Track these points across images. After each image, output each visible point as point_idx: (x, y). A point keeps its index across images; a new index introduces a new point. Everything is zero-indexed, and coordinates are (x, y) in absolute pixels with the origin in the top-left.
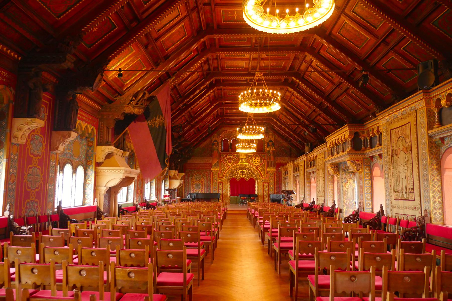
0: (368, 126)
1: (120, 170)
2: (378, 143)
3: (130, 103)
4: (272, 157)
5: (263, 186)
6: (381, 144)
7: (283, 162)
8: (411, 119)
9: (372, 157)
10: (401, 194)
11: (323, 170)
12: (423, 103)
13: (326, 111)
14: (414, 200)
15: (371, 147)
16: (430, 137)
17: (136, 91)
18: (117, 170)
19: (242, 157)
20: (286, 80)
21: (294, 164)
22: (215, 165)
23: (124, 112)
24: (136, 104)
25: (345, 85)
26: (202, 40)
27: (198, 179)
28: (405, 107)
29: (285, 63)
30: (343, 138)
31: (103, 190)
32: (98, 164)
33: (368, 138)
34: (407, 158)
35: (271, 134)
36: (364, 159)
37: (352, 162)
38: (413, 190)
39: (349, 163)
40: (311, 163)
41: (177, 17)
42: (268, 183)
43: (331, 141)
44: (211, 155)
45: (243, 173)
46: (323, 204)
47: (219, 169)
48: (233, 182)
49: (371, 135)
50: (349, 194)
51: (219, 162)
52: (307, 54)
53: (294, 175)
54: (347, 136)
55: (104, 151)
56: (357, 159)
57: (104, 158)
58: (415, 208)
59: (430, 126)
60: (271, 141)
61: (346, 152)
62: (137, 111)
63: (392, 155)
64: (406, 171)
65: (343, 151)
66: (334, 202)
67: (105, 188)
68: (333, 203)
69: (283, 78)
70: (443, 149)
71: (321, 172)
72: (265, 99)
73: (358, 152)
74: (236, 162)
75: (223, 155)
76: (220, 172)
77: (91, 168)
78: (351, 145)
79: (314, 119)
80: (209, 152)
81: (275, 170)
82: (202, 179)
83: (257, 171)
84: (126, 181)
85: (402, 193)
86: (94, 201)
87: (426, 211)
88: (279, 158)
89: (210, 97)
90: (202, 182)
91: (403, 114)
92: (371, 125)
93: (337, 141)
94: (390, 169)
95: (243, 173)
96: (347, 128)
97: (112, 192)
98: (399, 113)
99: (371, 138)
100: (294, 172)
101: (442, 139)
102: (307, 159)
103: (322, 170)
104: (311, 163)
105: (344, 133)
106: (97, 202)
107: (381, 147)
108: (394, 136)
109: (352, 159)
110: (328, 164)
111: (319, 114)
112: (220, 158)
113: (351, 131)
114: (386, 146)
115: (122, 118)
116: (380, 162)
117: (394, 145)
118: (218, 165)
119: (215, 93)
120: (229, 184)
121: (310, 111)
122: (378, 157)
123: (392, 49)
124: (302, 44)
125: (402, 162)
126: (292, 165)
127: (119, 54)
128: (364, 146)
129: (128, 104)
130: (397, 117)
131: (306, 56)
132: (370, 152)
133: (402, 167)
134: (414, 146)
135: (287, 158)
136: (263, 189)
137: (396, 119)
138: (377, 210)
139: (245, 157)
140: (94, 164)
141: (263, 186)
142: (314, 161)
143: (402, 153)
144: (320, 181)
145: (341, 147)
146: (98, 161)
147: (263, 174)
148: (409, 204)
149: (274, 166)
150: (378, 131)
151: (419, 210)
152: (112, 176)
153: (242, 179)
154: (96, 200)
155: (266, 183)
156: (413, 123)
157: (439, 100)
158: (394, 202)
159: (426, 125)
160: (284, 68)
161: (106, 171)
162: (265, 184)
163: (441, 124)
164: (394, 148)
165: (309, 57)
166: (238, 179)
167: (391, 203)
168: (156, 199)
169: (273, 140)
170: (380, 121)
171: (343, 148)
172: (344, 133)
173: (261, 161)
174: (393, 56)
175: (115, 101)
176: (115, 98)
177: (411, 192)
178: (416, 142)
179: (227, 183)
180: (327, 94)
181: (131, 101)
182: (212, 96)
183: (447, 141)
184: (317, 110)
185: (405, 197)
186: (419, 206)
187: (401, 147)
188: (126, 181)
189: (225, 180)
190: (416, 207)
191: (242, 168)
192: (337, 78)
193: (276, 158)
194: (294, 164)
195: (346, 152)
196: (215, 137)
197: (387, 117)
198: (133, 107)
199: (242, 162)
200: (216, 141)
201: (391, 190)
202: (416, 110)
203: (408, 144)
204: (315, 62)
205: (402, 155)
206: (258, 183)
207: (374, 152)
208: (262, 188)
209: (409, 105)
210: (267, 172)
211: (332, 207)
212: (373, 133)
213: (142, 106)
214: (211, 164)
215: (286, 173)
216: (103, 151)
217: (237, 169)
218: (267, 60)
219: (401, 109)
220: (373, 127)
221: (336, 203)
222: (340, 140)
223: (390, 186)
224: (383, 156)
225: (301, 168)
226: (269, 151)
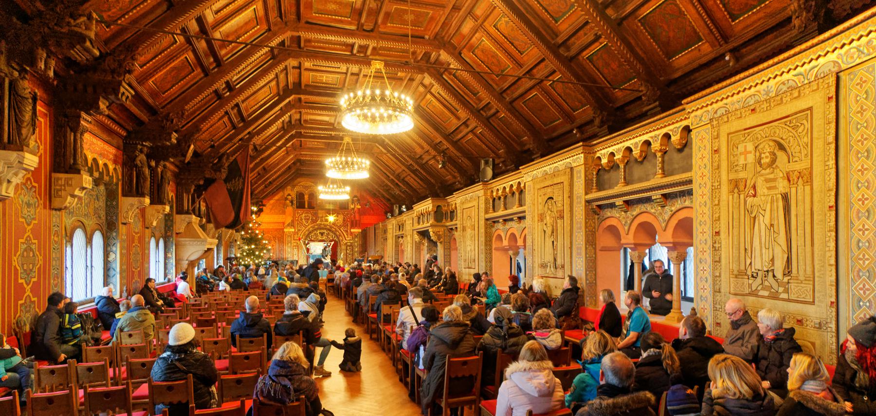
8: (475, 203)
12: (481, 193)
13: (414, 172)
15: (452, 220)
31: (185, 264)
38: (474, 261)
45: (322, 234)
59: (486, 212)
76: (295, 233)
97: (192, 264)
110: (415, 232)
142: (403, 225)
150: (456, 208)
172: (427, 205)
173: (344, 220)
174: (470, 136)
191: (321, 229)
200: (289, 195)
210: (351, 233)
214: (284, 223)
216: (181, 222)
225: (390, 231)
226: (353, 209)
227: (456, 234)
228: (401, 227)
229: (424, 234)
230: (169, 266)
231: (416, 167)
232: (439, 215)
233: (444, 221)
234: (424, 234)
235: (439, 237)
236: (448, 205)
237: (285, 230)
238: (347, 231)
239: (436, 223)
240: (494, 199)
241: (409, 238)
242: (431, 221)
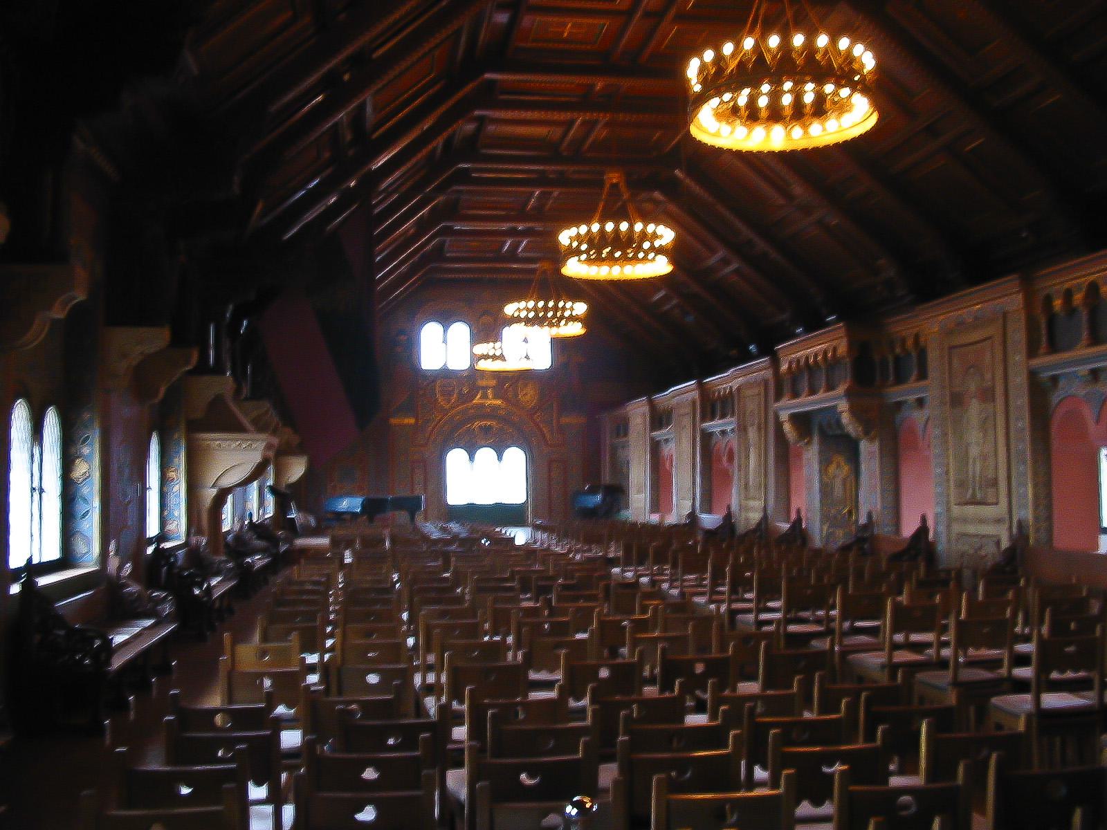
6: (923, 375)
9: (899, 405)
10: (970, 491)
11: (759, 429)
14: (997, 504)
15: (900, 379)
16: (1033, 375)
19: (483, 383)
21: (652, 404)
31: (210, 493)
32: (195, 427)
33: (891, 359)
38: (994, 483)
39: (845, 418)
47: (412, 421)
49: (898, 350)
53: (652, 439)
59: (1032, 352)
65: (830, 387)
70: (1055, 399)
71: (752, 434)
72: (626, 246)
85: (974, 490)
87: (1020, 522)
91: (976, 318)
94: (946, 434)
99: (897, 359)
101: (1055, 380)
103: (755, 427)
108: (956, 363)
110: (784, 416)
116: (919, 417)
126: (646, 409)
132: (896, 393)
134: (999, 390)
137: (961, 326)
138: (909, 528)
139: (493, 383)
140: (183, 426)
141: (550, 471)
144: (747, 457)
151: (1007, 526)
152: (233, 459)
156: (998, 340)
157: (1048, 300)
158: (956, 510)
159: (1023, 346)
163: (1053, 348)
183: (1062, 383)
185: (979, 496)
186: (1007, 517)
195: (841, 390)
197: (941, 318)
199: (485, 396)
201: (948, 480)
202: (1005, 315)
205: (974, 409)
207: (905, 393)
215: (622, 428)
217: (472, 419)
222: (819, 358)
230: (172, 500)
240: (1052, 319)
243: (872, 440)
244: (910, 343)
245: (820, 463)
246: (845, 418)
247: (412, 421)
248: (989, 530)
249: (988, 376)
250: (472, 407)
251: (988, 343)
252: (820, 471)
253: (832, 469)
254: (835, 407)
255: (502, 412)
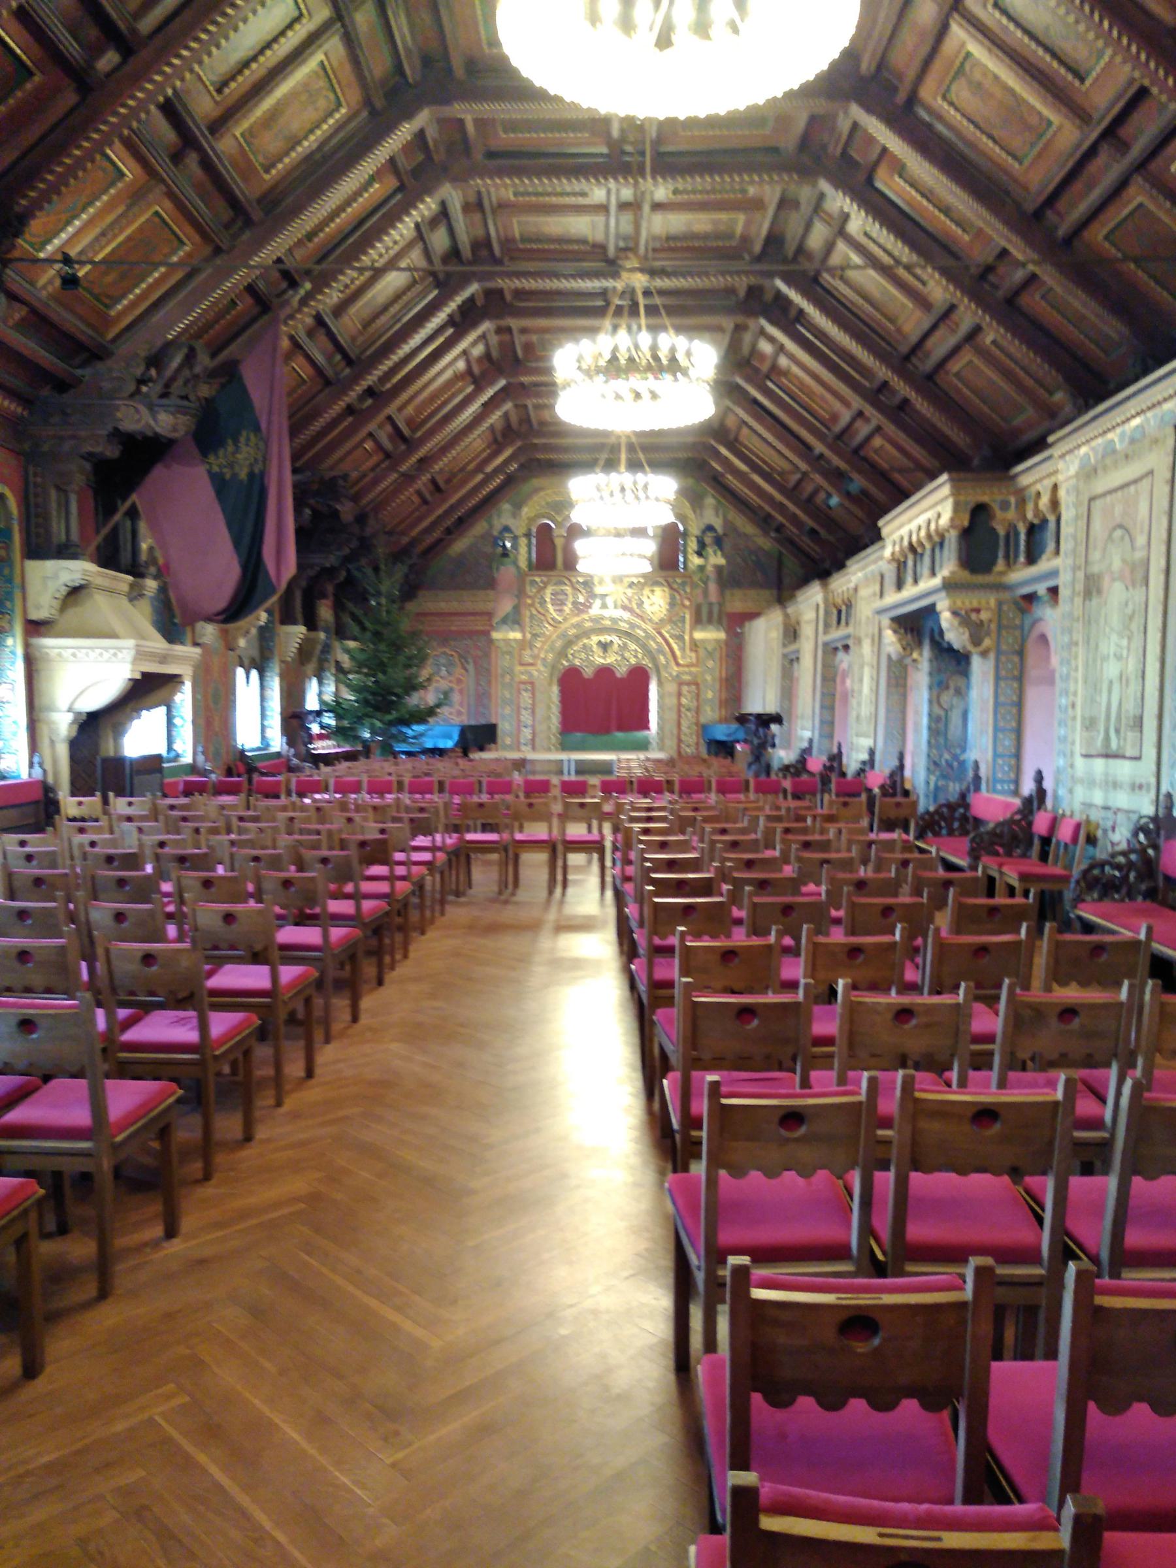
0: (1024, 480)
1: (119, 649)
2: (1051, 546)
3: (138, 391)
4: (713, 587)
5: (680, 694)
6: (1057, 552)
7: (749, 607)
9: (1031, 598)
13: (900, 412)
14: (1138, 758)
17: (159, 343)
18: (106, 649)
20: (754, 292)
21: (787, 616)
22: (504, 621)
23: (116, 429)
24: (165, 395)
25: (968, 315)
26: (405, 132)
27: (443, 672)
28: (1143, 411)
29: (748, 223)
30: (933, 527)
32: (35, 628)
33: (1022, 530)
34: (1131, 606)
35: (710, 501)
36: (1000, 604)
37: (955, 613)
38: (1139, 723)
40: (840, 612)
41: (290, 26)
42: (697, 684)
43: (896, 536)
44: (491, 584)
46: (864, 763)
47: (517, 635)
48: (570, 681)
49: (1030, 515)
50: (952, 728)
51: (517, 609)
52: (824, 185)
53: (785, 656)
54: (945, 520)
55: (56, 576)
56: (975, 604)
57: (56, 604)
58: (1141, 787)
60: (710, 528)
61: (937, 581)
62: (165, 422)
63: (1088, 594)
64: (1125, 653)
66: (901, 758)
67: (70, 717)
68: (896, 763)
69: (741, 284)
73: (980, 579)
74: (579, 608)
75: (533, 582)
76: (523, 644)
77: (10, 641)
78: (960, 550)
79: (861, 446)
80: (480, 573)
81: (722, 635)
82: (458, 671)
83: (660, 639)
84: (147, 689)
86: (31, 765)
88: (738, 593)
89: (468, 362)
90: (459, 681)
91: (1133, 441)
92: (1033, 476)
93: (914, 538)
94: (1076, 644)
95: (605, 647)
96: (946, 490)
98: (1123, 435)
100: (784, 645)
102: (826, 600)
104: (840, 612)
105: (939, 508)
106: (41, 765)
107: (1057, 562)
108: (1097, 525)
109: (959, 603)
110: (886, 622)
111: (878, 429)
112: (521, 593)
113: (962, 498)
114: (1070, 561)
115: (112, 452)
117: (1096, 555)
118: (514, 619)
119: (487, 346)
120: (555, 689)
121: (846, 416)
122: (1046, 598)
123: (1141, 166)
124: (805, 142)
125: (1115, 620)
127: (49, 201)
128: (1007, 557)
129: (132, 396)
130: (1114, 451)
131: (822, 196)
133: (1114, 637)
135: (767, 594)
136: (680, 705)
140: (18, 629)
141: (680, 694)
142: (849, 605)
143: (1118, 586)
145: (927, 559)
146: (34, 615)
147: (678, 653)
148: (1124, 769)
149: (720, 622)
150: (1055, 504)
153: (605, 672)
154: (36, 759)
155: (689, 684)
160: (745, 239)
161: (67, 653)
162: (685, 689)
164: (1095, 569)
165: (838, 201)
166: (588, 672)
167: (1072, 766)
168: (286, 747)
169: (718, 524)
170: (1061, 465)
171: (933, 562)
173: (672, 604)
175: (79, 381)
176: (79, 372)
177: (1132, 728)
178: (1163, 548)
179: (550, 684)
180: (904, 349)
181: (141, 381)
182: (480, 360)
184: (869, 410)
185: (1114, 745)
186: (1153, 780)
187: (1117, 564)
188: (147, 689)
189: (540, 672)
190: (1143, 781)
192: (938, 290)
193: (728, 593)
194: (787, 616)
196: (503, 515)
198: (151, 407)
199: (604, 606)
200: (506, 529)
201: (1074, 718)
203: (1139, 555)
204: (859, 222)
205: (1116, 594)
206: (660, 684)
208: (675, 701)
209: (1154, 406)
210: (695, 645)
211: (892, 775)
212: (1036, 505)
213: (186, 403)
214: (489, 615)
217: (587, 634)
218: (665, 212)
219: (1128, 420)
220: (1039, 487)
221: (908, 762)
223: (1073, 706)
224: (1064, 593)
225: (807, 632)
226: (701, 568)
227: (1051, 618)
228: (841, 613)
229: (915, 625)
231: (903, 389)
232: (981, 544)
233: (1000, 565)
234: (915, 625)
235: (977, 632)
236: (1022, 502)
237: (496, 635)
238: (680, 638)
239: (965, 575)
241: (867, 649)
242: (948, 567)
243: (984, 654)
244: (1045, 501)
245: (930, 688)
246: (946, 618)
247: (517, 635)
248: (1122, 800)
249: (1141, 540)
250: (591, 620)
251: (1145, 483)
252: (930, 702)
253: (946, 698)
254: (933, 606)
255: (624, 626)
